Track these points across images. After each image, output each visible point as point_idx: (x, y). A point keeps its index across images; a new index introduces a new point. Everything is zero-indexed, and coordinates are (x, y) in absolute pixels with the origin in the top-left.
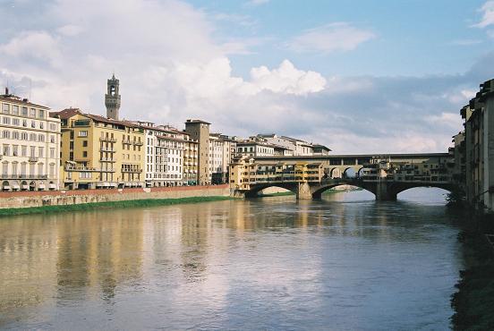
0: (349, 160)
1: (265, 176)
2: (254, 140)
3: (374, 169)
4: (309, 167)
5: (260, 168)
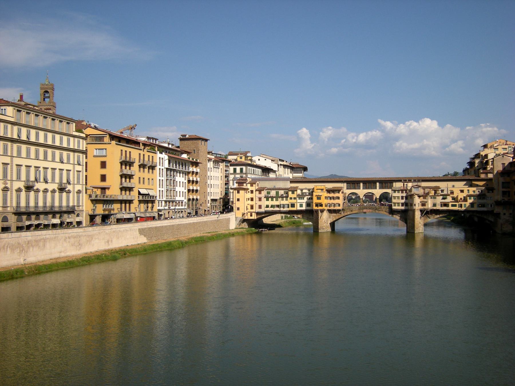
0: (369, 183)
1: (275, 203)
2: (243, 160)
3: (404, 195)
4: (329, 191)
5: (268, 193)
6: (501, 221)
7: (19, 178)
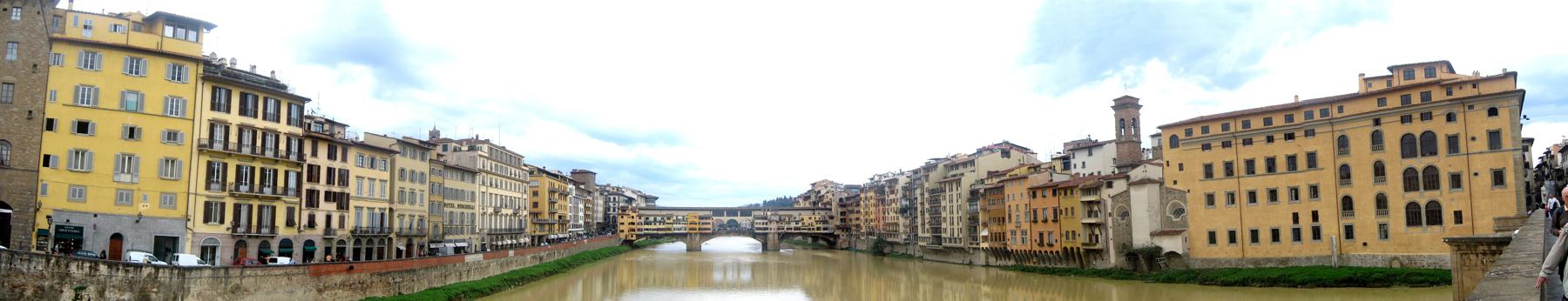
1: (653, 227)
2: (615, 190)
4: (701, 218)
6: (840, 241)
7: (491, 204)
